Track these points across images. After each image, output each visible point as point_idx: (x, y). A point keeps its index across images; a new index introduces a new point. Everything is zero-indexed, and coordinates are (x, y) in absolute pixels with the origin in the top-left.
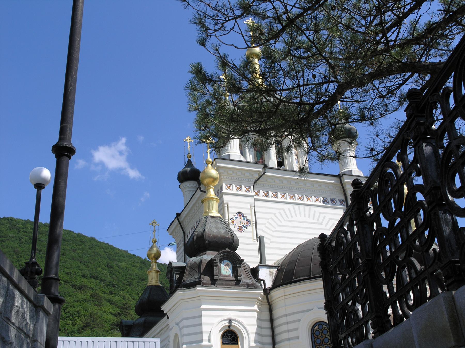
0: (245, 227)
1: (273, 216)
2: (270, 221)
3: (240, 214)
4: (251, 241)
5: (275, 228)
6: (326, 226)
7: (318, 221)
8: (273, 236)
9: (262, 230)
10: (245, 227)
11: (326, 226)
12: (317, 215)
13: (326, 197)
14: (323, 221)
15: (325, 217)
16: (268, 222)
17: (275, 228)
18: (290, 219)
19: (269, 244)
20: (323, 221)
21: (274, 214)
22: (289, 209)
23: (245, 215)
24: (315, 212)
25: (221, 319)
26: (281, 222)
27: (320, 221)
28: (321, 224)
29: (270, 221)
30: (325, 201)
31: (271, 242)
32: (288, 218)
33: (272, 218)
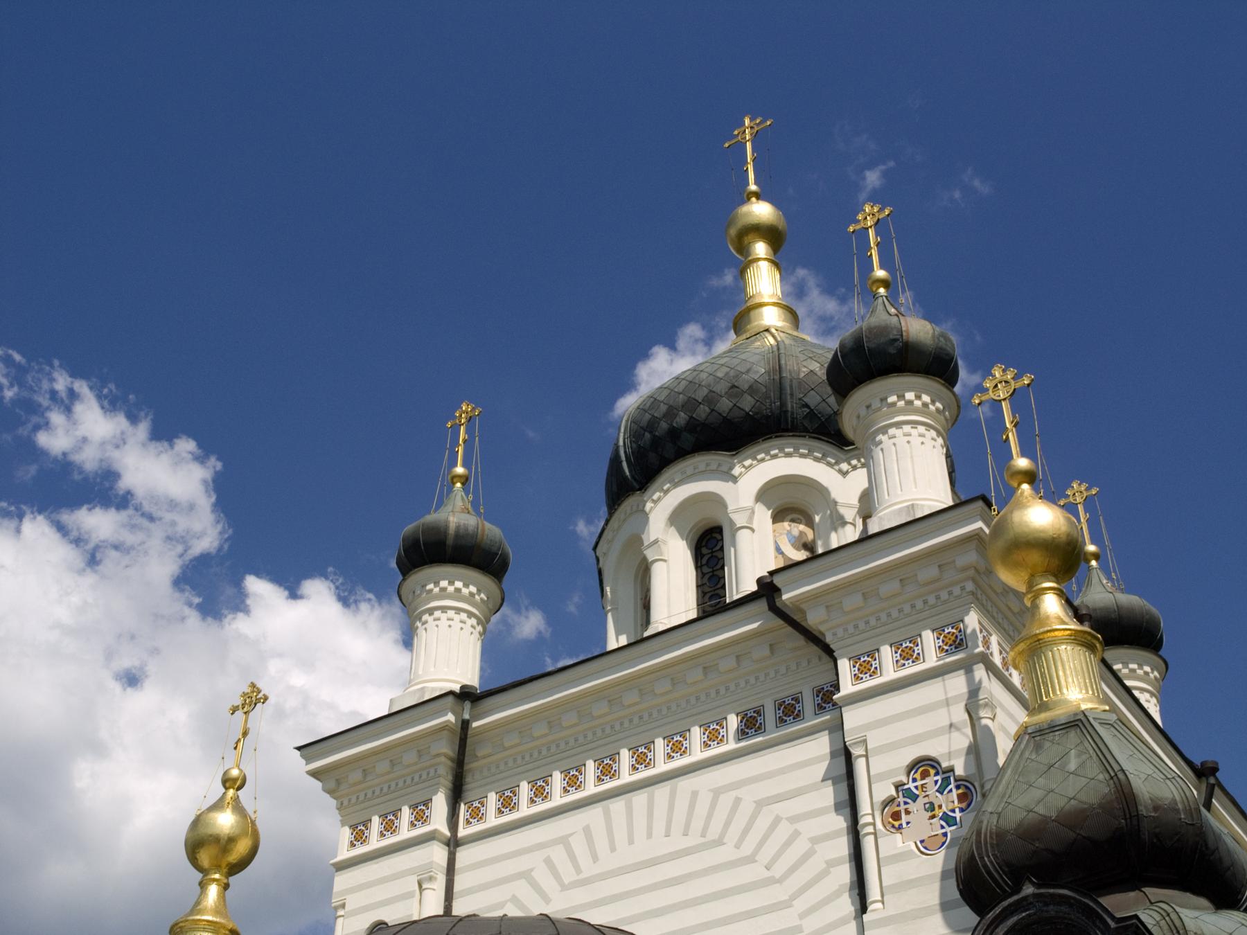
6: (737, 846)
7: (703, 835)
11: (737, 846)
12: (702, 809)
13: (750, 704)
14: (727, 824)
15: (738, 801)
18: (588, 869)
20: (727, 824)
21: (526, 875)
22: (587, 830)
24: (695, 794)
26: (546, 899)
27: (713, 833)
28: (719, 842)
30: (751, 724)
32: (578, 870)
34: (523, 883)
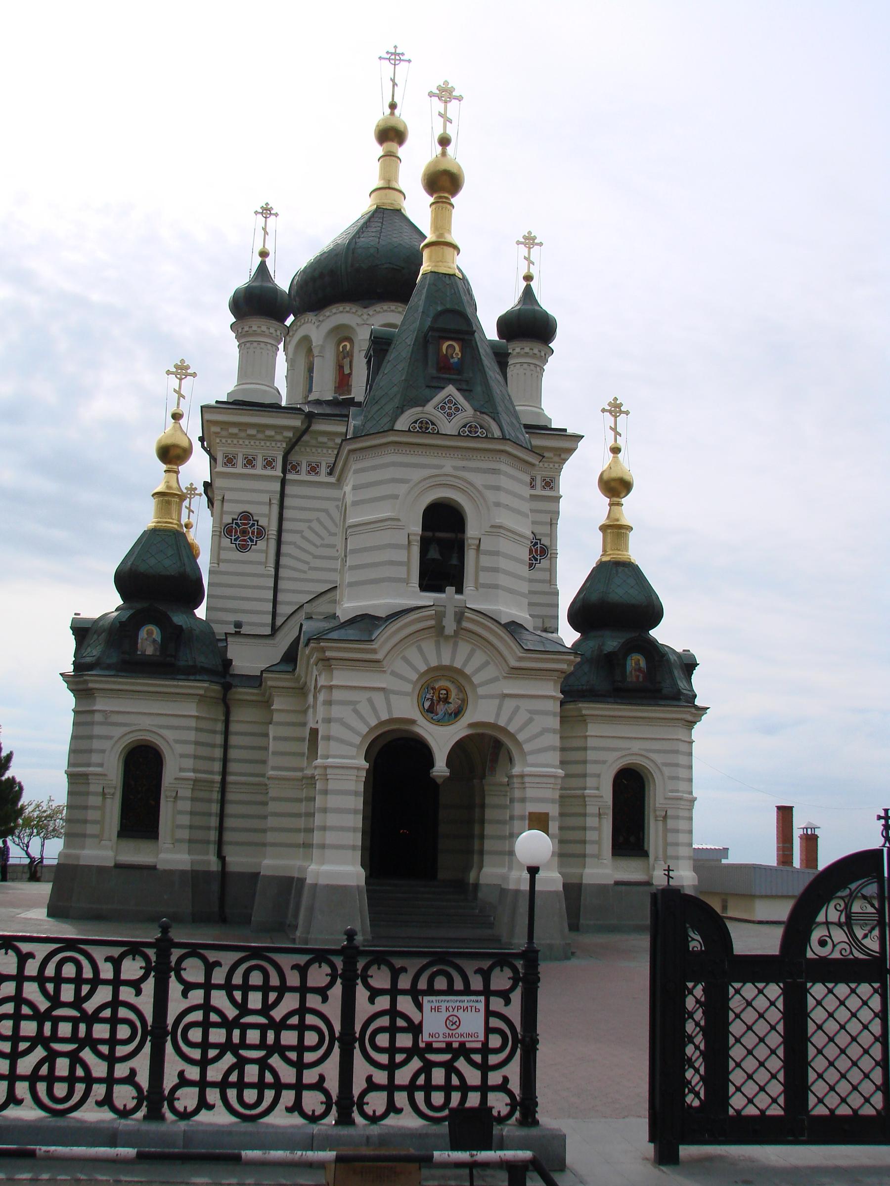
0: (252, 541)
1: (323, 516)
2: (315, 525)
3: (246, 516)
4: (260, 569)
5: (323, 539)
8: (315, 557)
9: (294, 544)
10: (252, 541)
16: (310, 528)
17: (323, 539)
19: (305, 572)
21: (326, 511)
23: (255, 518)
25: (128, 729)
29: (315, 525)
31: (310, 569)
33: (318, 520)
34: (324, 514)
